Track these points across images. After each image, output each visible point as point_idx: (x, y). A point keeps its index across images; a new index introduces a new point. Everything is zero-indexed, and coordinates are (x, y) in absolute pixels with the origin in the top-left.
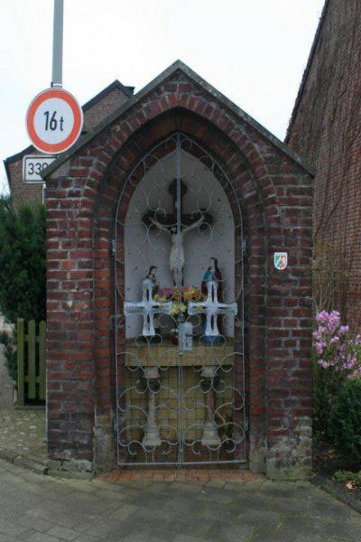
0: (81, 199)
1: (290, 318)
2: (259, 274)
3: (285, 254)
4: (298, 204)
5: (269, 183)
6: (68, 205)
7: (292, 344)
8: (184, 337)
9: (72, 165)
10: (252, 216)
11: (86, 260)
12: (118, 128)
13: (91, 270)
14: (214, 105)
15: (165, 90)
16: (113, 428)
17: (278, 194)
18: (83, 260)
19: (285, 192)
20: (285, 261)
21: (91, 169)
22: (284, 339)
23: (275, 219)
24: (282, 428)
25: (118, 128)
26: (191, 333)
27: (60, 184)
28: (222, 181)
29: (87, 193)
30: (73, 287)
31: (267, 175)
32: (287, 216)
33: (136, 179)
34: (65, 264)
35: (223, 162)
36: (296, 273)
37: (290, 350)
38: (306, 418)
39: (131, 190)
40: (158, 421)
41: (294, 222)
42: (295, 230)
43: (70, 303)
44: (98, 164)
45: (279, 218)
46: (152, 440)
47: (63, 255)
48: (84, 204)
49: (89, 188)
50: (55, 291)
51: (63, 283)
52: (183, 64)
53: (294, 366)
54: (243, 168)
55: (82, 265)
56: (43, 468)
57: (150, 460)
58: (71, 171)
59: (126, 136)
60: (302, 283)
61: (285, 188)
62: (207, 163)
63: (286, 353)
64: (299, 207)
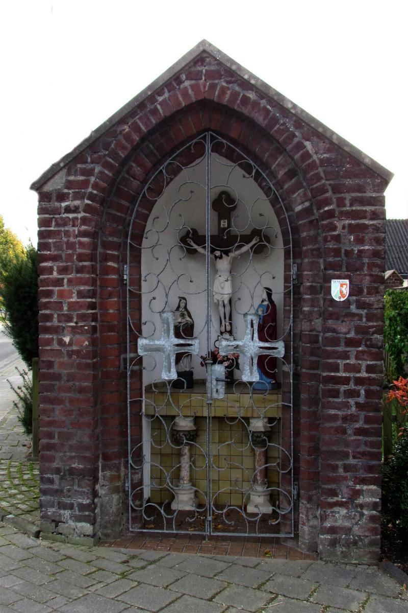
0: (80, 216)
1: (352, 361)
2: (312, 306)
3: (347, 281)
4: (365, 218)
5: (327, 191)
6: (65, 222)
7: (353, 394)
8: (214, 382)
9: (69, 174)
10: (305, 234)
11: (87, 288)
12: (126, 128)
13: (94, 300)
14: (251, 95)
15: (187, 79)
16: (124, 486)
17: (338, 206)
18: (82, 288)
19: (347, 202)
20: (346, 290)
21: (93, 179)
22: (343, 388)
23: (333, 237)
24: (339, 498)
25: (126, 128)
26: (223, 377)
27: (54, 198)
28: (267, 191)
29: (87, 209)
30: (70, 320)
31: (323, 181)
32: (350, 233)
33: (158, 191)
34: (61, 294)
35: (266, 166)
36: (361, 305)
37: (352, 401)
38: (373, 487)
39: (150, 206)
40: (193, 481)
41: (360, 241)
42: (360, 251)
43: (67, 339)
44: (101, 172)
45: (339, 236)
46: (184, 501)
47: (59, 282)
48: (84, 221)
49: (90, 202)
50: (48, 324)
51: (58, 315)
52: (210, 45)
53: (357, 421)
54: (292, 174)
55: (80, 294)
56: (35, 529)
57: (170, 527)
58: (69, 182)
59: (136, 138)
60: (370, 318)
61: (348, 197)
62: (247, 169)
63: (347, 405)
64: (367, 222)
